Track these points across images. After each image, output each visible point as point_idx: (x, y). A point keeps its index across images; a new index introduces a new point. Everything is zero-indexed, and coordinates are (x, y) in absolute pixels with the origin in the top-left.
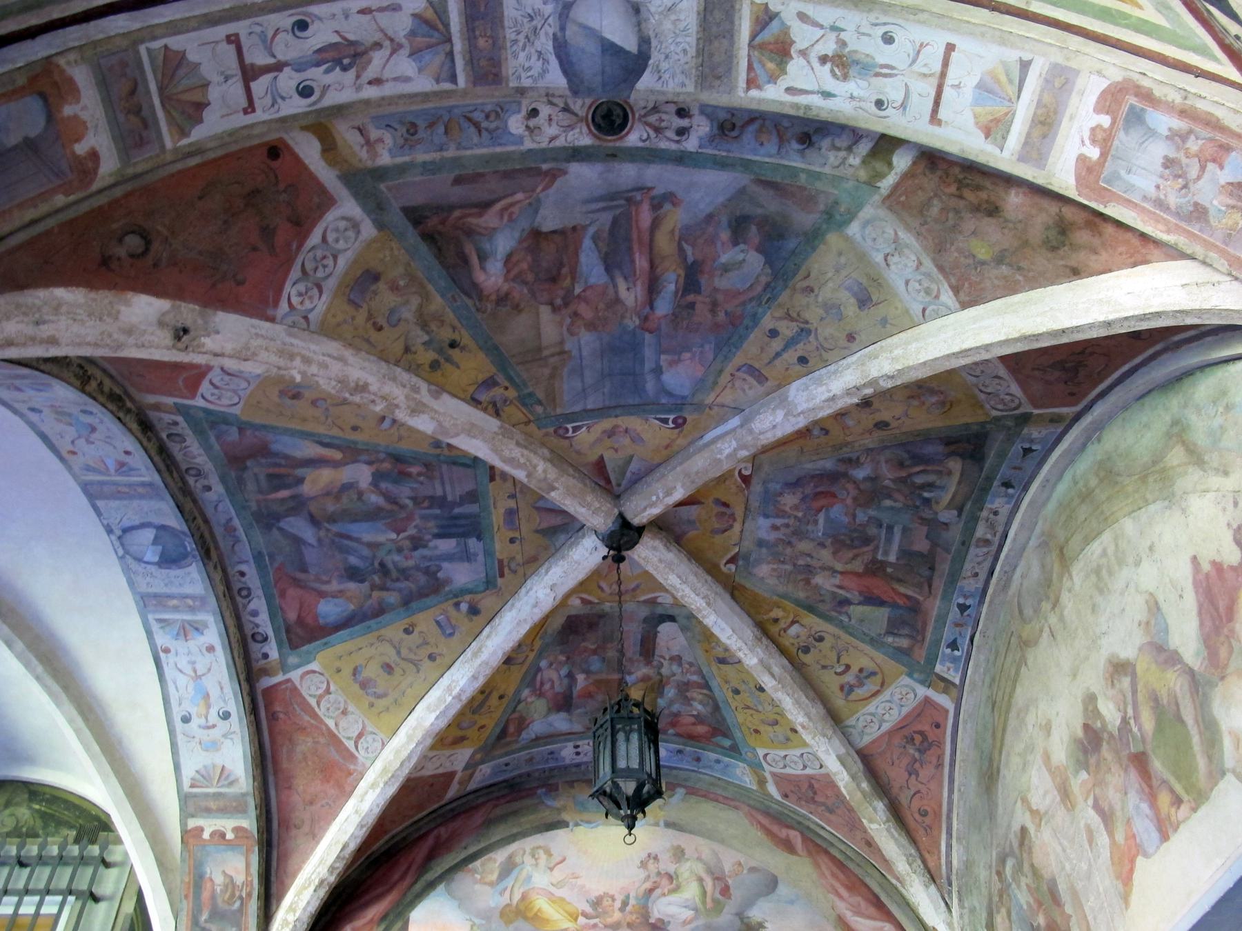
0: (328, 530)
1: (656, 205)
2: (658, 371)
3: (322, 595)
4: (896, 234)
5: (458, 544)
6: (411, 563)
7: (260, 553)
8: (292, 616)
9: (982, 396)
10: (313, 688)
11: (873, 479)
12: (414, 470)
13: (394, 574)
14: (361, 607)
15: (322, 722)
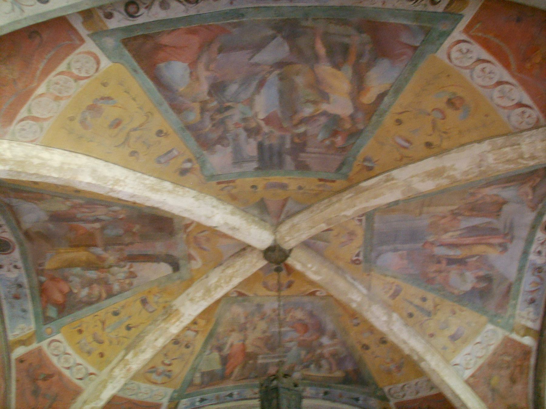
0: (270, 73)
1: (500, 245)
2: (395, 250)
3: (193, 65)
4: (492, 344)
5: (252, 157)
6: (230, 125)
7: (243, 15)
8: (166, 40)
9: (401, 385)
10: (78, 65)
11: (321, 345)
12: (339, 140)
13: (219, 117)
14: (181, 96)
15: (41, 80)
